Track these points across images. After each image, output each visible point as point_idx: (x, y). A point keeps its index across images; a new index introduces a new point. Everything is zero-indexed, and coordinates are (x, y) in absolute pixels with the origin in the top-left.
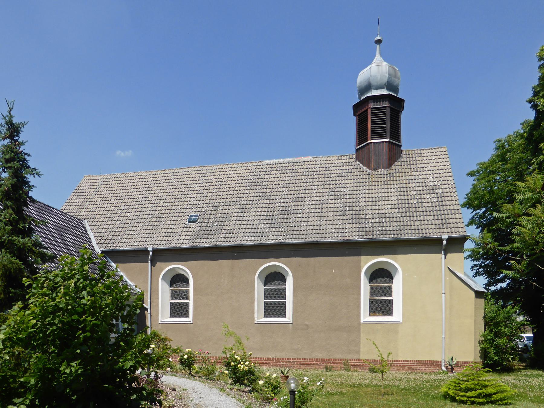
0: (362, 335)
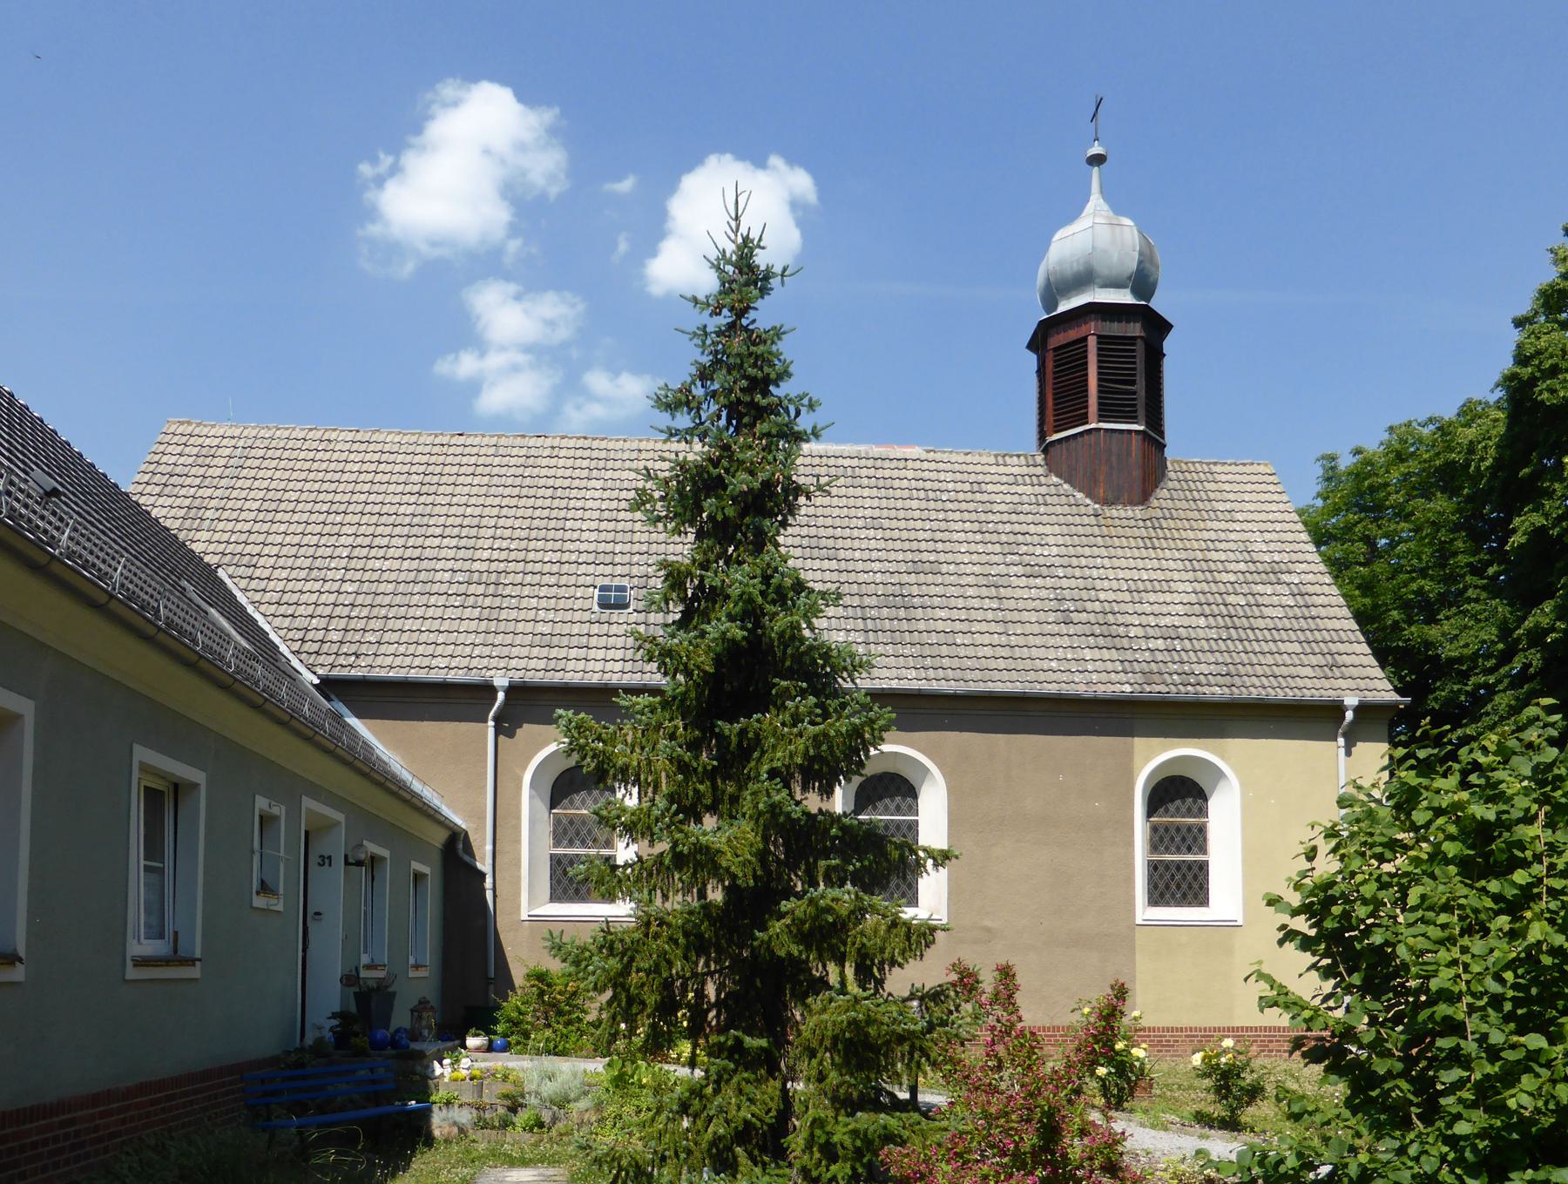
0: (1138, 957)
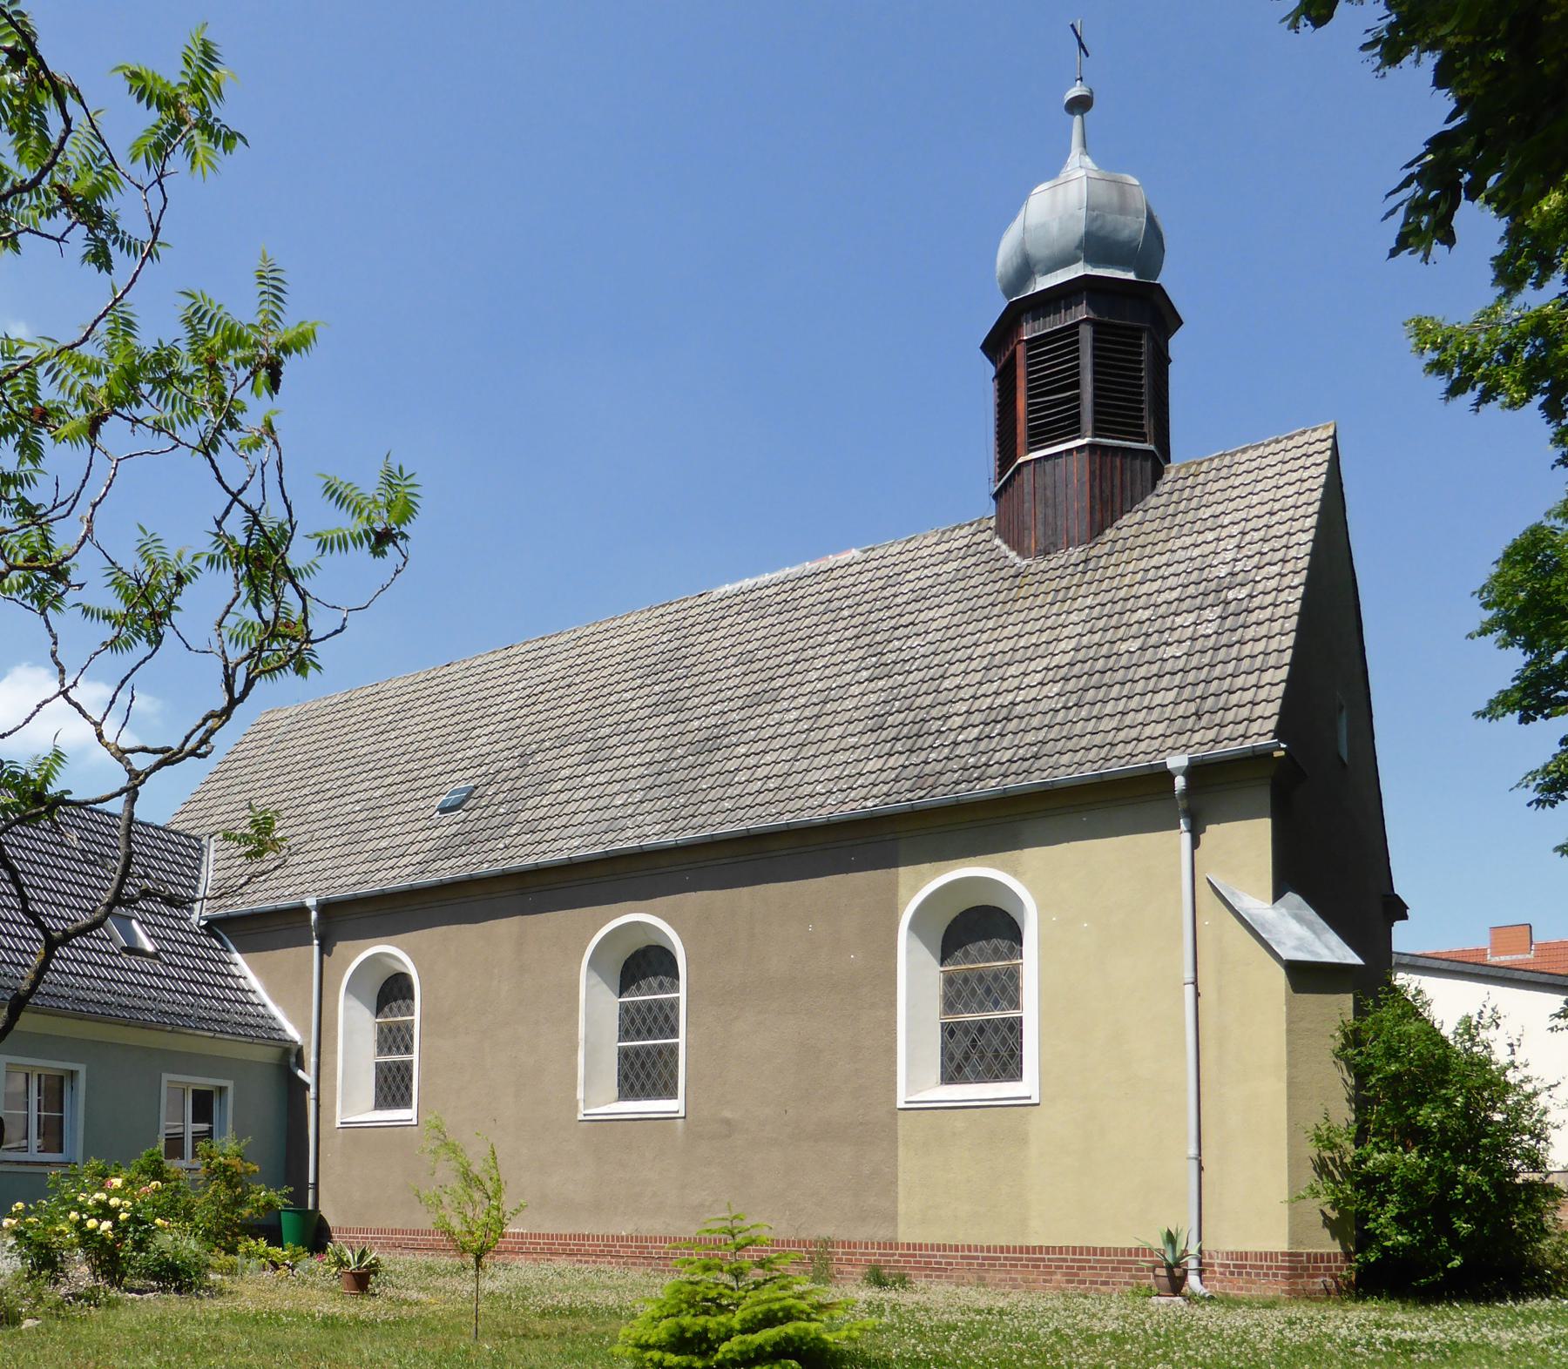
0: (901, 1152)
